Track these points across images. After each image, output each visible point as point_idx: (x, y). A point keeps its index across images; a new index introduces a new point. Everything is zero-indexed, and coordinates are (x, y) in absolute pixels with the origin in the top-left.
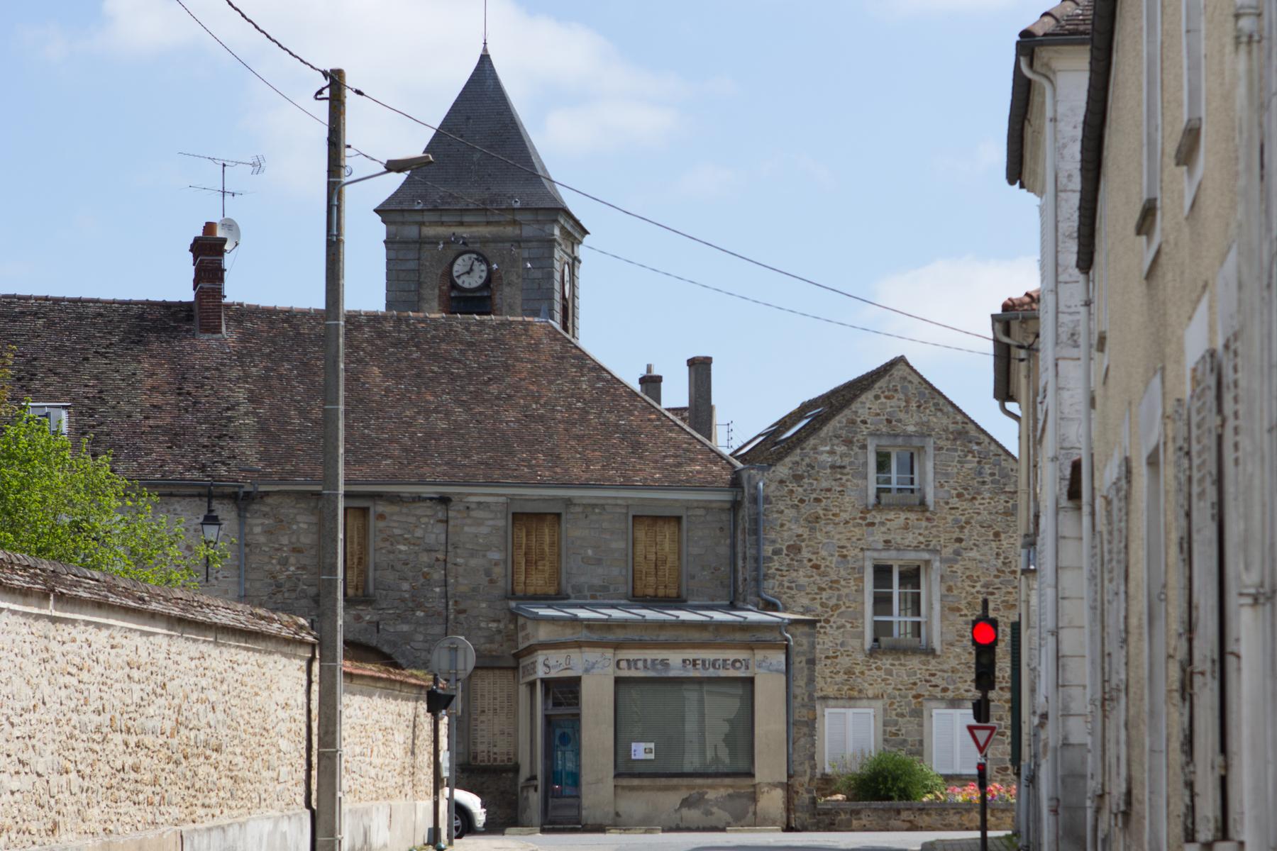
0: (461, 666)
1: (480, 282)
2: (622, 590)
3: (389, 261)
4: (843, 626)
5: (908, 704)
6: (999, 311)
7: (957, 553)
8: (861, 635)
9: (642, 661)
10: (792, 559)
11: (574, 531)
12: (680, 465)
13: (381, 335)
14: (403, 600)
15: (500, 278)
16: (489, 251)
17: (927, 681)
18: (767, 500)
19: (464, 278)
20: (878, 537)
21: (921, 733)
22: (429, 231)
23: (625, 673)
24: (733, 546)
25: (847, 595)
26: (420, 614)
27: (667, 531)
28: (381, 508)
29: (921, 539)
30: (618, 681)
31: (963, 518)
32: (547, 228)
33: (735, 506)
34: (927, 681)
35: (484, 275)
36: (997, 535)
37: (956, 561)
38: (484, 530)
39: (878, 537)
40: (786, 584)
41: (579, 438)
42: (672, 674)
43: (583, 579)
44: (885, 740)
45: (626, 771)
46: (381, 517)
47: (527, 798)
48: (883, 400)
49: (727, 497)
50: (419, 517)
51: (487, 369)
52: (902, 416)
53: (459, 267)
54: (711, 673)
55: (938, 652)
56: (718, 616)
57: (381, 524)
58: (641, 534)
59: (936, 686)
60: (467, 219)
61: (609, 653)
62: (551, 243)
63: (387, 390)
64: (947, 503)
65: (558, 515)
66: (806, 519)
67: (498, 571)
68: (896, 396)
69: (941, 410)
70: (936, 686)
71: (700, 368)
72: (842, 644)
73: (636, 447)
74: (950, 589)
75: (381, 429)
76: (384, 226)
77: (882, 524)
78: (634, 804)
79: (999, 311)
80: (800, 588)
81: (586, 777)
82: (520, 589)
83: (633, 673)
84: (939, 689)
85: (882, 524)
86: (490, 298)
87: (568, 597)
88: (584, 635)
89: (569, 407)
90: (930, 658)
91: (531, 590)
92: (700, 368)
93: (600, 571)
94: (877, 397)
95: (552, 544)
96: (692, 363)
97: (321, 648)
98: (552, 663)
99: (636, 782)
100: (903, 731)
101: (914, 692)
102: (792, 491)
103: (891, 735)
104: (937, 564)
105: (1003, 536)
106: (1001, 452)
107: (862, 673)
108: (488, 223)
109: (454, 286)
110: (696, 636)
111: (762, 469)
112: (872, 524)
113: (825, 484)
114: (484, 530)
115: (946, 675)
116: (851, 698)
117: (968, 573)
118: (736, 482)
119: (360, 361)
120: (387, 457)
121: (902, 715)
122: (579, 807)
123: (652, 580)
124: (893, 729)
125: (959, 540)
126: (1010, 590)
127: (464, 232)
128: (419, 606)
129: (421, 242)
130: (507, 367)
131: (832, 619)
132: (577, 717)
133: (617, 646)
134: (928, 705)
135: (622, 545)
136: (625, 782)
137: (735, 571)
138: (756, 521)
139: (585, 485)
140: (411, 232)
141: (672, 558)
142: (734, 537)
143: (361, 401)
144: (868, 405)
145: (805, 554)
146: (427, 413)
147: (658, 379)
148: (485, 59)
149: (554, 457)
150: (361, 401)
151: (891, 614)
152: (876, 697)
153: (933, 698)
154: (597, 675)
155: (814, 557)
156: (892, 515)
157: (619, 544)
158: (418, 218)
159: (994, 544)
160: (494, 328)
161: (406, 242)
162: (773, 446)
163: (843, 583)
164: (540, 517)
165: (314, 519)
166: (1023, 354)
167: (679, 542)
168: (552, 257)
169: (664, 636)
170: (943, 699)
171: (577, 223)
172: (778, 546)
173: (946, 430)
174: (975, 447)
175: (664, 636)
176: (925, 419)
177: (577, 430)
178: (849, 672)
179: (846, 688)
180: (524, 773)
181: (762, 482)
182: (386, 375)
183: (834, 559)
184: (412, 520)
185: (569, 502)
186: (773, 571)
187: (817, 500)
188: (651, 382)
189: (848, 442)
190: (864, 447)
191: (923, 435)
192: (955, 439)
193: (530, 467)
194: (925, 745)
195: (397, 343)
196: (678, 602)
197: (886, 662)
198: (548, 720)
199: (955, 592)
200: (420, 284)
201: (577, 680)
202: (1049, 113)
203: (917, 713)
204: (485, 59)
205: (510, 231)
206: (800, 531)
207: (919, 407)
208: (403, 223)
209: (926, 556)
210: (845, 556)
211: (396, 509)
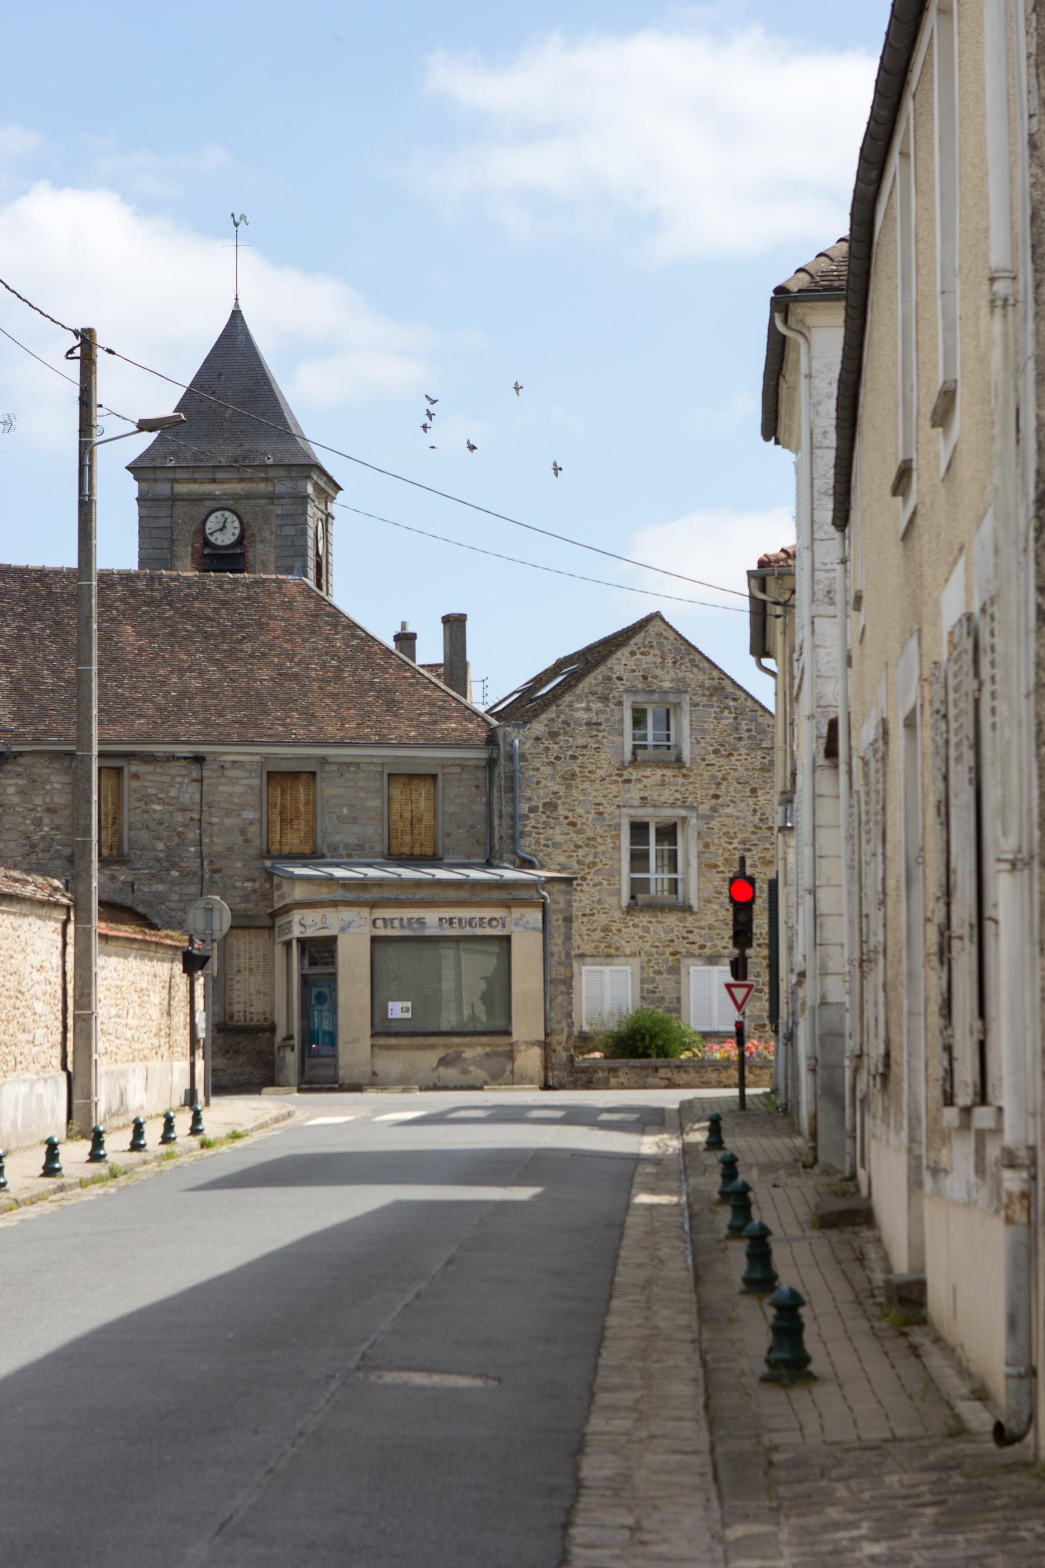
0: (216, 926)
1: (233, 539)
2: (378, 848)
3: (141, 518)
4: (600, 884)
5: (666, 961)
6: (754, 567)
7: (714, 809)
8: (618, 893)
9: (398, 920)
10: (548, 817)
11: (329, 789)
12: (435, 722)
13: (134, 593)
14: (158, 860)
15: (253, 535)
16: (242, 507)
17: (684, 938)
18: (523, 757)
19: (217, 535)
20: (634, 794)
21: (679, 991)
22: (182, 488)
23: (381, 932)
24: (489, 804)
25: (603, 852)
26: (175, 873)
27: (423, 789)
28: (135, 767)
29: (678, 795)
30: (374, 940)
31: (720, 775)
32: (300, 484)
33: (491, 763)
34: (684, 938)
35: (237, 532)
36: (754, 791)
37: (713, 818)
38: (238, 789)
39: (634, 794)
40: (543, 842)
41: (334, 696)
42: (428, 932)
43: (338, 838)
44: (643, 998)
45: (383, 1030)
46: (135, 776)
47: (283, 1058)
48: (639, 656)
49: (482, 754)
50: (173, 777)
51: (241, 627)
52: (658, 672)
53: (212, 524)
54: (468, 931)
55: (695, 909)
56: (475, 874)
57: (135, 784)
58: (396, 793)
59: (693, 943)
60: (219, 475)
61: (365, 912)
62: (305, 499)
63: (141, 649)
64: (704, 759)
65: (313, 774)
66: (562, 777)
67: (253, 830)
68: (652, 652)
69: (697, 666)
70: (693, 943)
71: (455, 626)
72: (599, 902)
73: (391, 706)
74: (707, 846)
75: (134, 688)
76: (136, 484)
77: (639, 780)
78: (391, 1064)
79: (754, 567)
80: (557, 845)
81: (343, 1036)
82: (275, 848)
83: (389, 932)
84: (696, 946)
85: (639, 780)
86: (243, 555)
87: (323, 856)
88: (339, 894)
89: (324, 666)
90: (687, 915)
91: (286, 849)
92: (455, 626)
93: (355, 829)
94: (633, 653)
95: (307, 803)
96: (447, 620)
97: (76, 910)
98: (308, 922)
99: (393, 1041)
100: (661, 988)
101: (671, 950)
102: (548, 749)
103: (648, 993)
104: (693, 821)
105: (760, 792)
106: (757, 707)
107: (619, 930)
109: (207, 543)
110: (452, 894)
111: (517, 726)
112: (629, 781)
113: (581, 741)
114: (238, 789)
115: (703, 932)
116: (608, 956)
117: (725, 830)
118: (492, 740)
119: (112, 620)
120: (140, 716)
121: (659, 973)
122: (336, 1066)
123: (407, 838)
124: (651, 987)
125: (716, 797)
126: (768, 846)
127: (216, 489)
128: (174, 866)
129: (174, 499)
130: (261, 626)
131: (589, 877)
132: (333, 977)
133: (373, 905)
134: (685, 962)
135: (377, 803)
136: (382, 1041)
137: (491, 828)
138: (511, 778)
139: (340, 744)
140: (164, 489)
141: (427, 817)
142: (490, 794)
143: (114, 660)
144: (623, 662)
145: (562, 811)
146: (181, 671)
147: (413, 637)
148: (236, 314)
149: (308, 716)
150: (114, 660)
151: (647, 871)
152: (633, 955)
153: (693, 955)
154: (353, 934)
155: (570, 814)
156: (648, 772)
157: (375, 803)
158: (171, 475)
159: (751, 801)
160: (247, 586)
161: (157, 500)
162: (527, 704)
163: (599, 840)
164: (294, 775)
165: (67, 779)
166: (779, 610)
167: (435, 800)
168: (305, 513)
169: (421, 894)
170: (700, 956)
171: (330, 479)
172: (534, 803)
173: (702, 686)
174: (732, 703)
175: (421, 894)
176: (681, 675)
177: (330, 689)
178: (606, 929)
179: (603, 945)
180: (281, 1033)
181: (518, 738)
182: (139, 634)
183: (591, 816)
184: (167, 779)
185: (324, 761)
186: (528, 829)
187: (574, 757)
188: (406, 640)
189: (604, 699)
190: (620, 704)
191: (679, 692)
192: (711, 695)
193: (284, 725)
194: (683, 1002)
195: (151, 602)
196: (434, 860)
197: (643, 919)
198: (305, 980)
199: (712, 849)
200: (172, 541)
201: (332, 940)
202: (804, 369)
203: (675, 970)
204: (236, 314)
205: (262, 487)
206: (556, 788)
207: (675, 663)
208: (156, 480)
209: (683, 813)
210: (601, 814)
211: (149, 768)
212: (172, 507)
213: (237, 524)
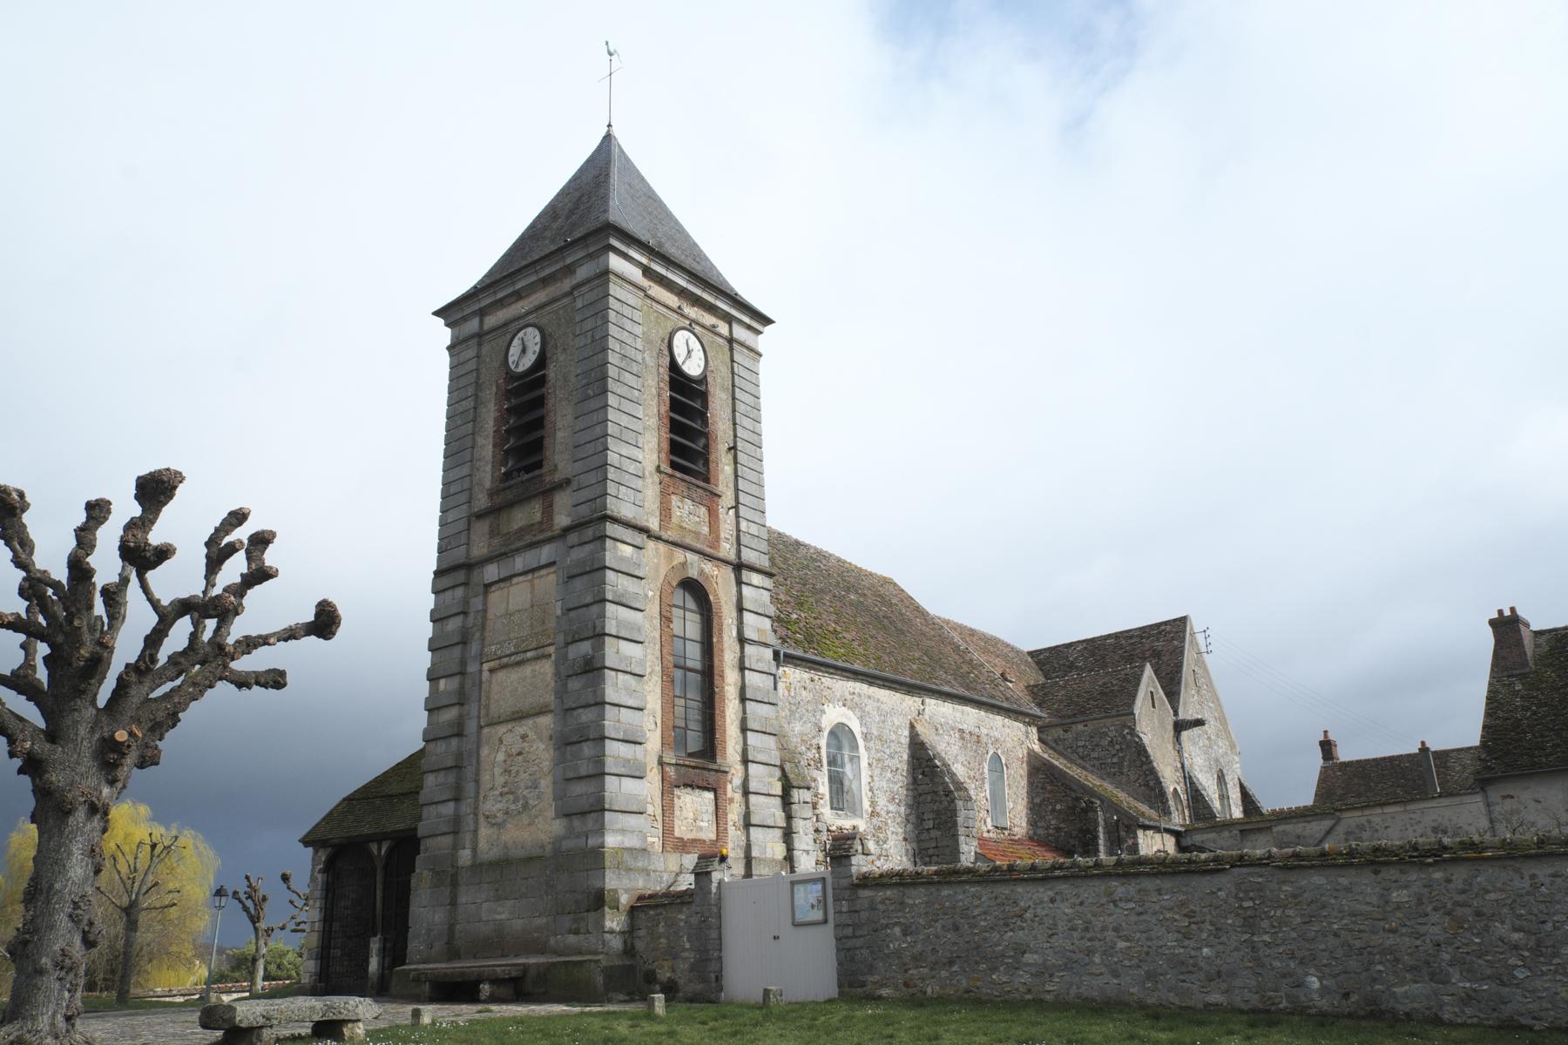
22: (491, 321)
35: (537, 349)
76: (449, 330)
108: (545, 282)
140: (473, 326)
148: (608, 138)
212: (480, 344)
213: (538, 339)
